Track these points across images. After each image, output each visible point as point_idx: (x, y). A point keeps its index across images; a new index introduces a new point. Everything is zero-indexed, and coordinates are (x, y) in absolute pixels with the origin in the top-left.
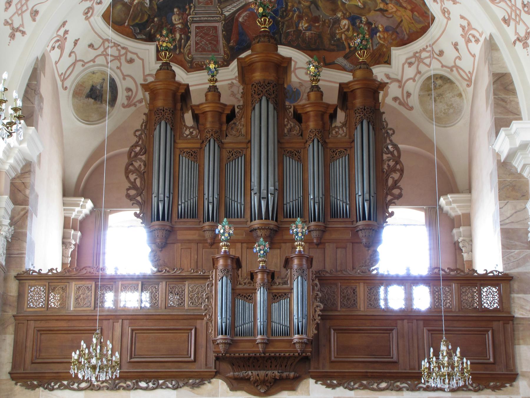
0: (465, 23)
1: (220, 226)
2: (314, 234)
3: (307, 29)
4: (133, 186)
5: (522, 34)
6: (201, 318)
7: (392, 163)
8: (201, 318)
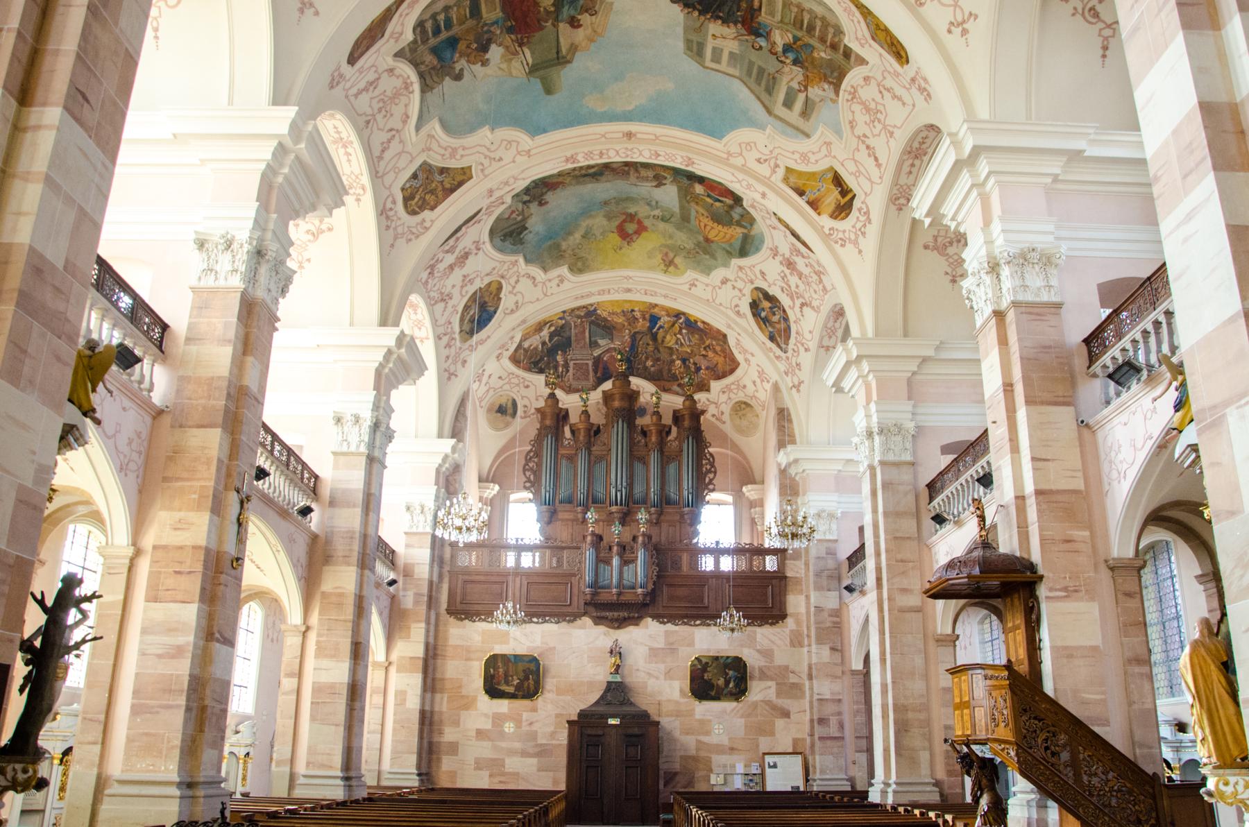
1: (589, 513)
2: (654, 516)
3: (652, 366)
4: (529, 480)
5: (796, 383)
6: (575, 575)
7: (708, 467)
8: (575, 575)
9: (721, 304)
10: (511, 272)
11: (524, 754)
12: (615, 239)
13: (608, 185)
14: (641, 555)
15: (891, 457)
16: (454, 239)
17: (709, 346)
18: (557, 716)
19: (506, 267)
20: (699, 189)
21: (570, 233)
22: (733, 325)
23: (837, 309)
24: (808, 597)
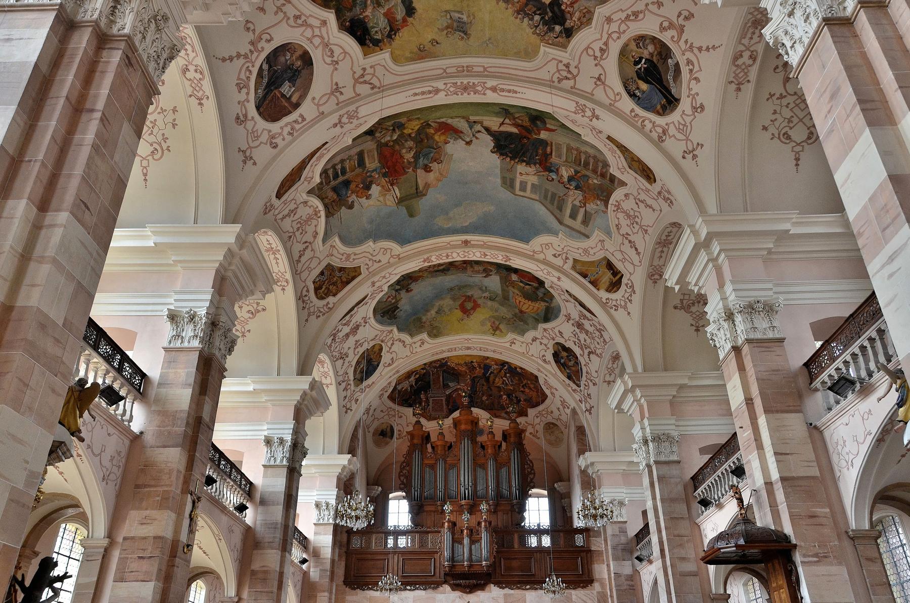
0: (562, 399)
2: (492, 507)
3: (487, 400)
4: (403, 483)
6: (437, 552)
7: (529, 470)
8: (437, 552)
10: (388, 338)
12: (458, 313)
13: (453, 277)
14: (484, 535)
17: (525, 385)
20: (514, 277)
21: (428, 311)
22: (542, 370)
23: (614, 355)
24: (608, 566)
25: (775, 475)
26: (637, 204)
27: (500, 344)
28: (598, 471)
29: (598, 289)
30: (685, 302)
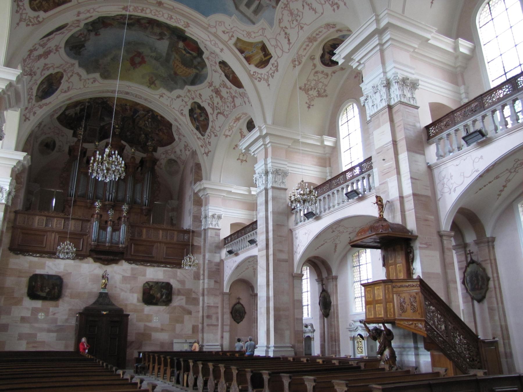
1: (97, 203)
5: (207, 151)
6: (86, 235)
9: (174, 108)
11: (49, 331)
14: (123, 228)
15: (275, 185)
16: (47, 38)
18: (70, 310)
19: (67, 66)
20: (181, 45)
24: (204, 256)
25: (408, 190)
26: (303, 6)
27: (152, 95)
28: (207, 194)
29: (249, 64)
30: (307, 86)
